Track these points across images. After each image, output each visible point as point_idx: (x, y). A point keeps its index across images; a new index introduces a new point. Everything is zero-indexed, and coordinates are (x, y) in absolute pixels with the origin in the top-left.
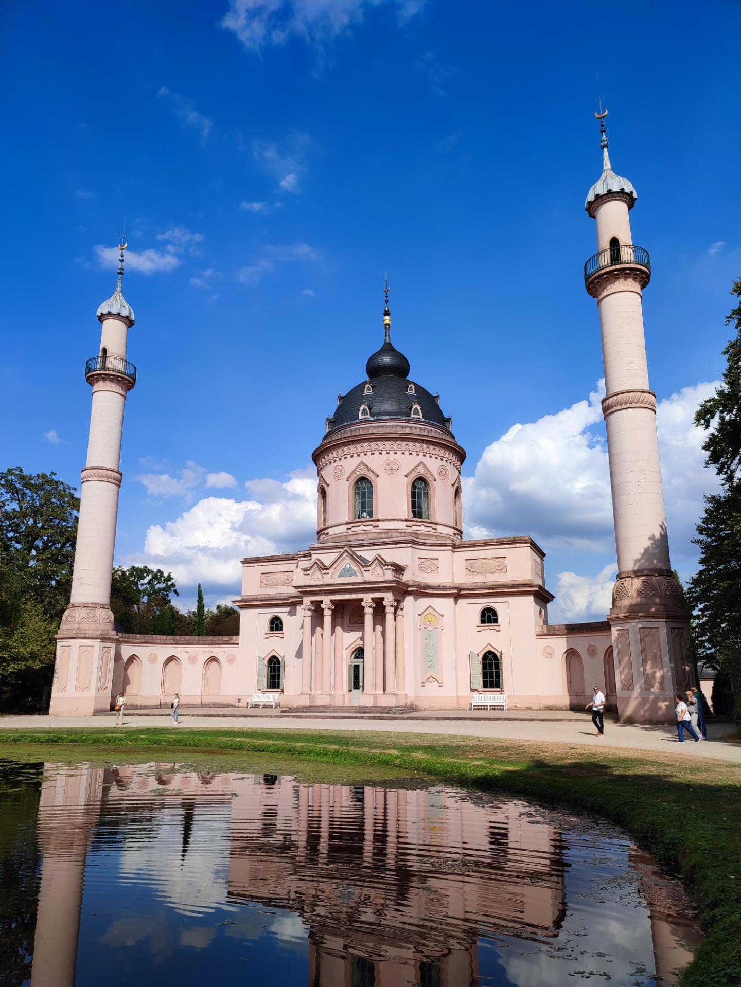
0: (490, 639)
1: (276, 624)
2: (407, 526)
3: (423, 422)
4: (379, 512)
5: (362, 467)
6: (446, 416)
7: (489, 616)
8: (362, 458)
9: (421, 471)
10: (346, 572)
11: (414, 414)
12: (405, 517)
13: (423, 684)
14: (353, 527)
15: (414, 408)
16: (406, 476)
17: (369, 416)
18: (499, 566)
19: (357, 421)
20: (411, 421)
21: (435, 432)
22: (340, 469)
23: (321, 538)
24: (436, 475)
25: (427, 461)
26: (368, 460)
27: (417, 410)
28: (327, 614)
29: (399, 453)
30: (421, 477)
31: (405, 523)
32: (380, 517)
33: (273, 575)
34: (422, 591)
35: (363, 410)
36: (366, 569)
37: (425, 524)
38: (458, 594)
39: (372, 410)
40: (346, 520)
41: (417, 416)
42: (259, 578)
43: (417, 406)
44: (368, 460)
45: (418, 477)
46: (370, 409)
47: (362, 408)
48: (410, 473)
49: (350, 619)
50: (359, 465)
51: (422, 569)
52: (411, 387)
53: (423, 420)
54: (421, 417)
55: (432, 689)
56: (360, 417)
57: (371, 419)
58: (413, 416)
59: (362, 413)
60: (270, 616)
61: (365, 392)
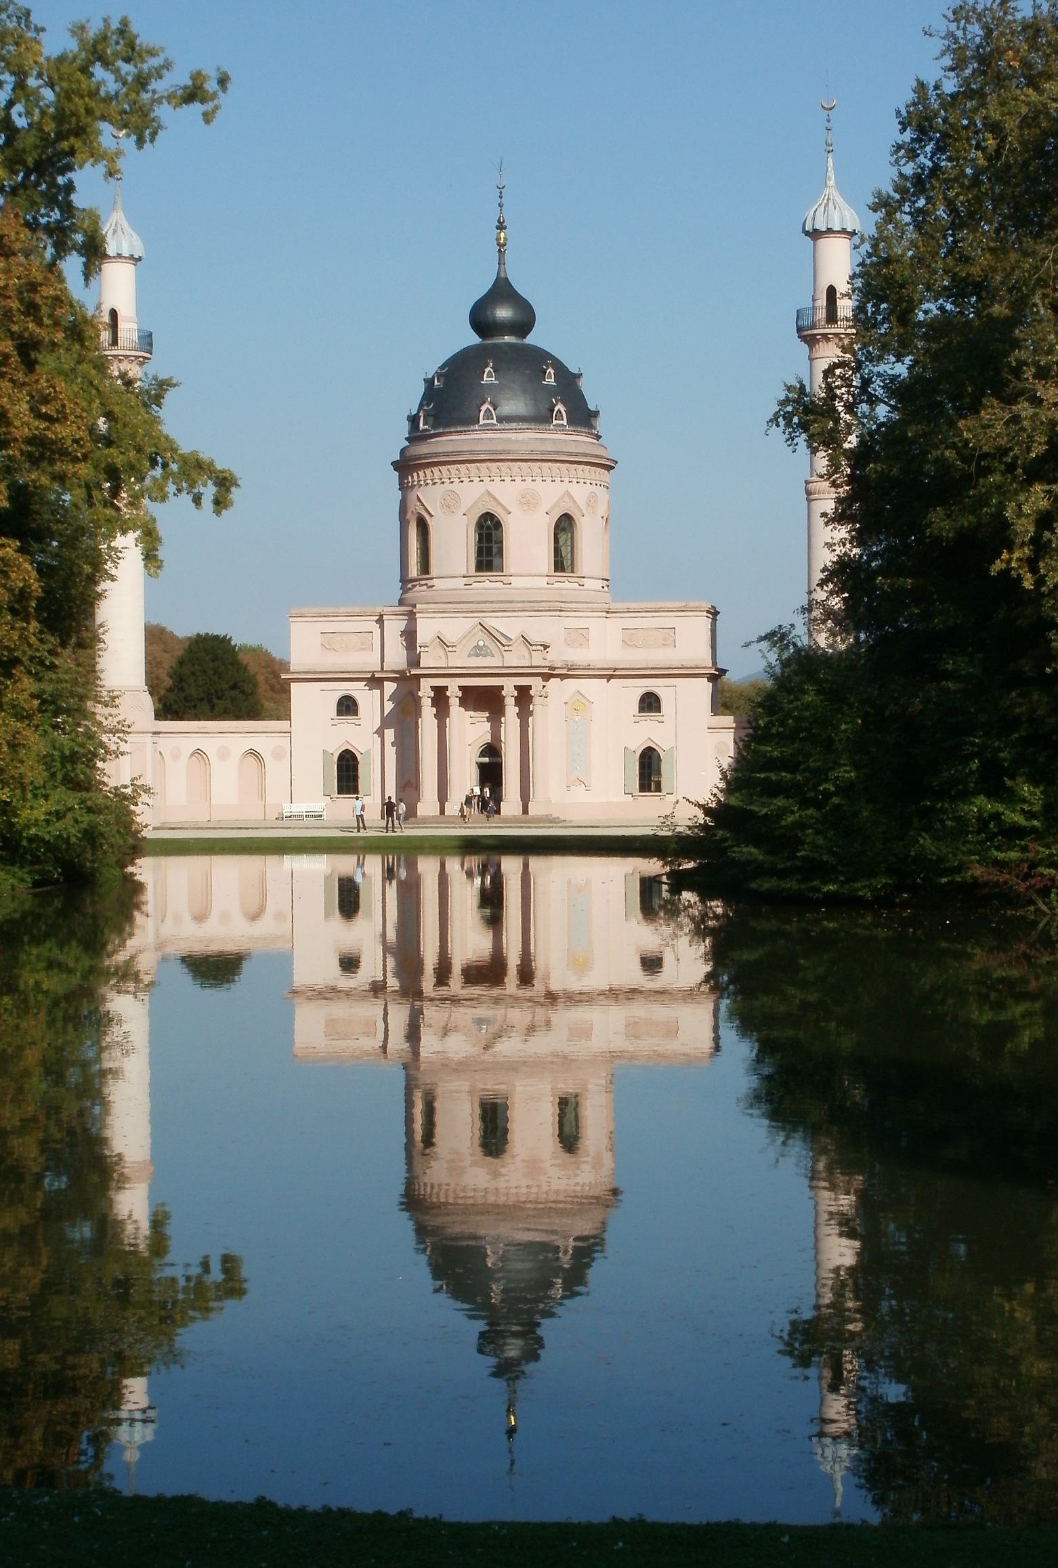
0: (649, 731)
1: (347, 706)
5: (488, 499)
6: (592, 407)
7: (650, 703)
10: (479, 651)
12: (545, 571)
15: (556, 409)
17: (494, 421)
18: (665, 639)
19: (477, 427)
22: (456, 497)
24: (583, 506)
26: (496, 488)
28: (454, 702)
29: (539, 479)
32: (512, 571)
33: (338, 637)
34: (568, 673)
36: (506, 648)
38: (611, 675)
40: (465, 573)
41: (561, 422)
42: (319, 639)
43: (560, 407)
47: (484, 408)
55: (579, 795)
56: (482, 422)
58: (555, 422)
60: (340, 694)
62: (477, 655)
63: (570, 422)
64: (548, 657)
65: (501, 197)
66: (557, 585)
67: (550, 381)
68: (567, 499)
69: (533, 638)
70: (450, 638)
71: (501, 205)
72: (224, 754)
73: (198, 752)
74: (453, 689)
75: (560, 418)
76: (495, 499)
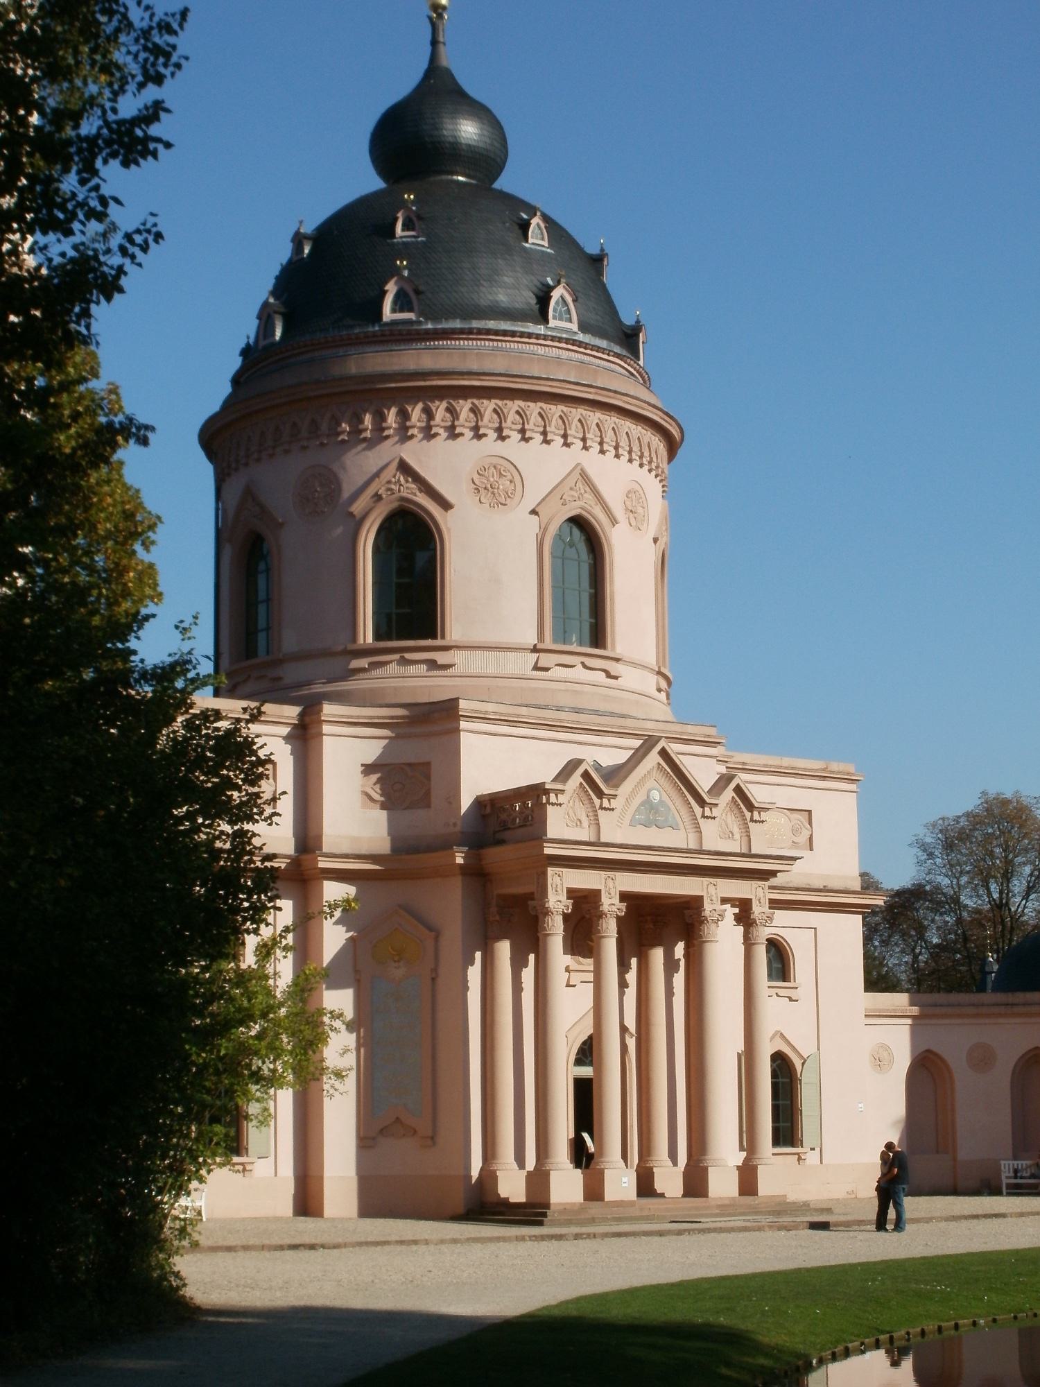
4: (456, 625)
15: (556, 294)
16: (534, 512)
20: (545, 337)
25: (595, 463)
44: (414, 453)
46: (417, 292)
47: (391, 288)
53: (581, 337)
54: (574, 327)
56: (388, 314)
59: (395, 302)
63: (583, 327)
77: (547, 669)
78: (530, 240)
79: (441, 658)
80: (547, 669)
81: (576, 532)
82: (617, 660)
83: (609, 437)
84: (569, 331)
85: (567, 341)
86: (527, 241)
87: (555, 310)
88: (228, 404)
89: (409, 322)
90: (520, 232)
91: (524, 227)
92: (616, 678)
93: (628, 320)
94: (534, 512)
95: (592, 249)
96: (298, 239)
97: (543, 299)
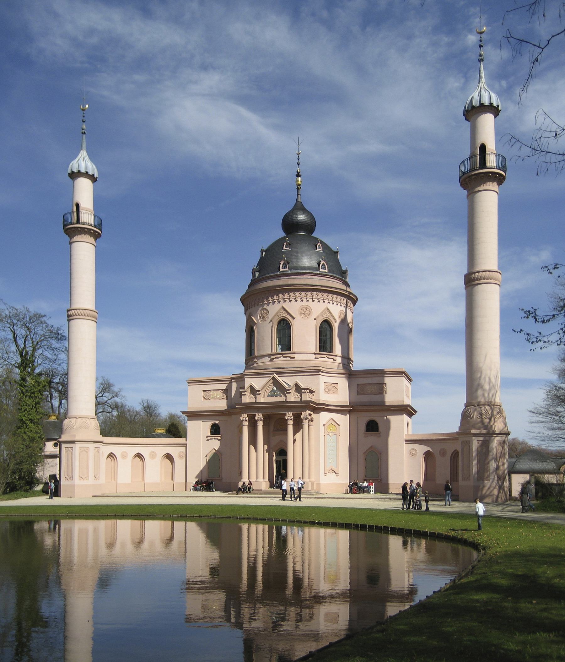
1: (215, 430)
2: (315, 358)
3: (328, 275)
4: (296, 346)
8: (282, 304)
9: (327, 316)
11: (321, 269)
12: (314, 351)
13: (326, 475)
14: (276, 358)
15: (322, 263)
16: (315, 319)
20: (319, 274)
21: (337, 284)
23: (249, 364)
26: (287, 305)
27: (324, 265)
29: (311, 300)
30: (326, 319)
31: (314, 356)
33: (212, 393)
35: (283, 264)
37: (328, 356)
39: (289, 264)
40: (269, 352)
44: (287, 305)
45: (324, 319)
47: (282, 263)
48: (318, 317)
49: (274, 427)
50: (280, 309)
51: (326, 391)
52: (319, 245)
53: (328, 274)
54: (326, 271)
57: (290, 272)
58: (321, 270)
59: (282, 266)
61: (284, 248)
62: (272, 396)
64: (313, 397)
65: (298, 159)
66: (320, 359)
67: (320, 250)
68: (327, 312)
69: (302, 385)
70: (257, 387)
71: (298, 164)
72: (153, 456)
73: (139, 456)
74: (259, 416)
75: (324, 268)
76: (287, 311)
77: (318, 358)
78: (318, 249)
79: (292, 356)
80: (318, 358)
81: (326, 324)
82: (336, 356)
83: (335, 299)
84: (326, 272)
85: (324, 275)
86: (316, 249)
87: (321, 267)
88: (247, 292)
89: (286, 271)
90: (315, 246)
91: (316, 245)
92: (336, 360)
93: (344, 268)
94: (315, 319)
95: (336, 250)
96: (262, 251)
97: (319, 264)
